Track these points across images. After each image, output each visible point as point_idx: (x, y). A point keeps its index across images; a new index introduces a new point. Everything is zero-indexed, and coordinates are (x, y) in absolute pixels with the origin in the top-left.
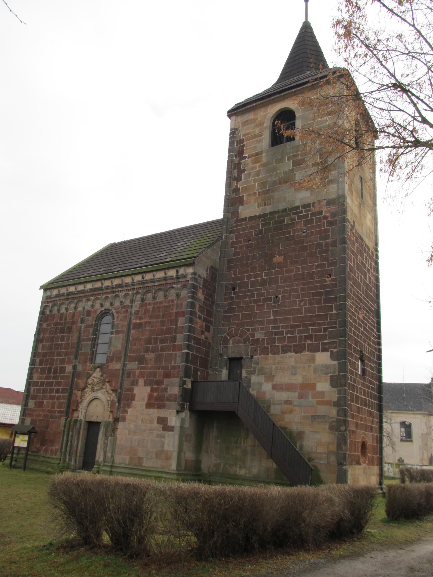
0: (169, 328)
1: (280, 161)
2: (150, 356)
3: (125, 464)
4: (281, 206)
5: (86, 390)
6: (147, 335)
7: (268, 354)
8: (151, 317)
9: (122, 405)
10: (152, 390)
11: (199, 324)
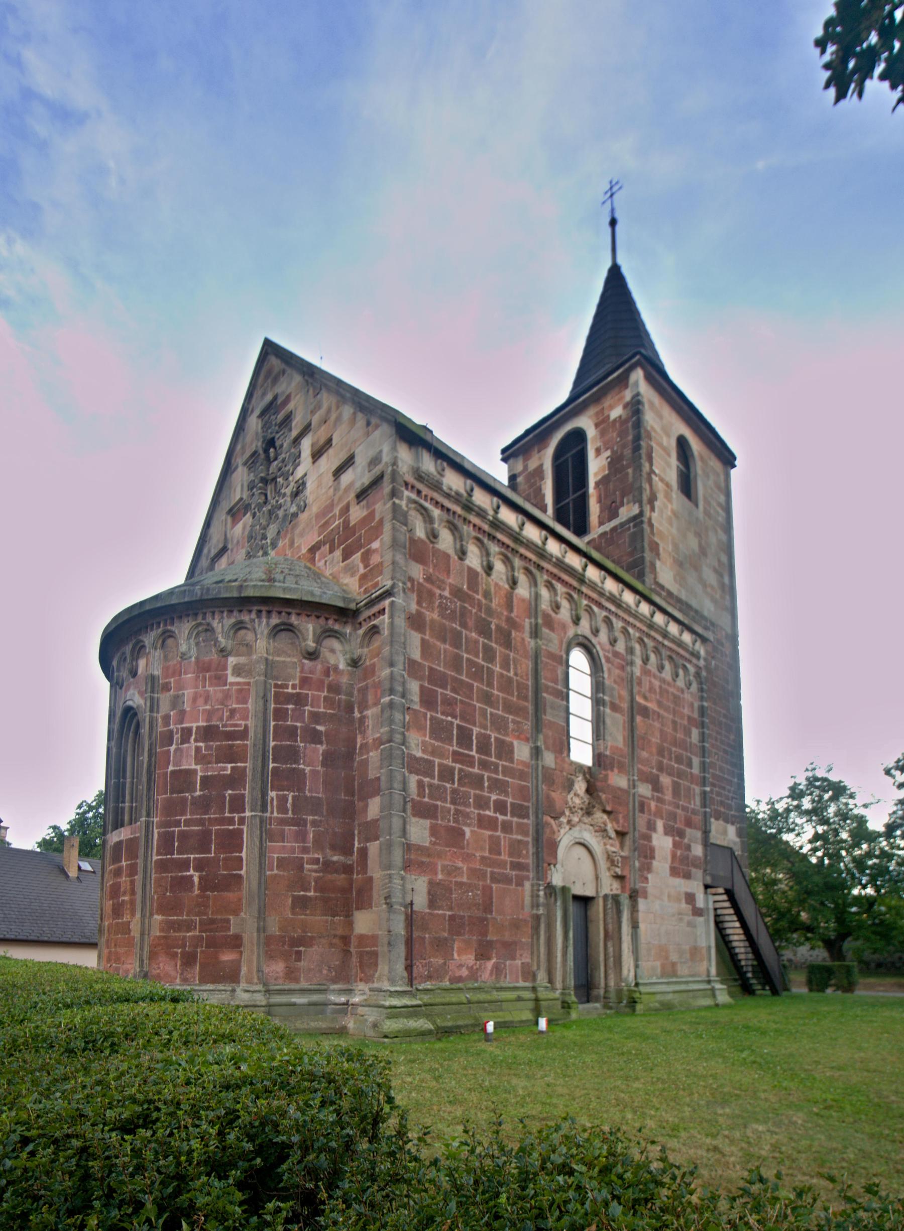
10: (676, 845)
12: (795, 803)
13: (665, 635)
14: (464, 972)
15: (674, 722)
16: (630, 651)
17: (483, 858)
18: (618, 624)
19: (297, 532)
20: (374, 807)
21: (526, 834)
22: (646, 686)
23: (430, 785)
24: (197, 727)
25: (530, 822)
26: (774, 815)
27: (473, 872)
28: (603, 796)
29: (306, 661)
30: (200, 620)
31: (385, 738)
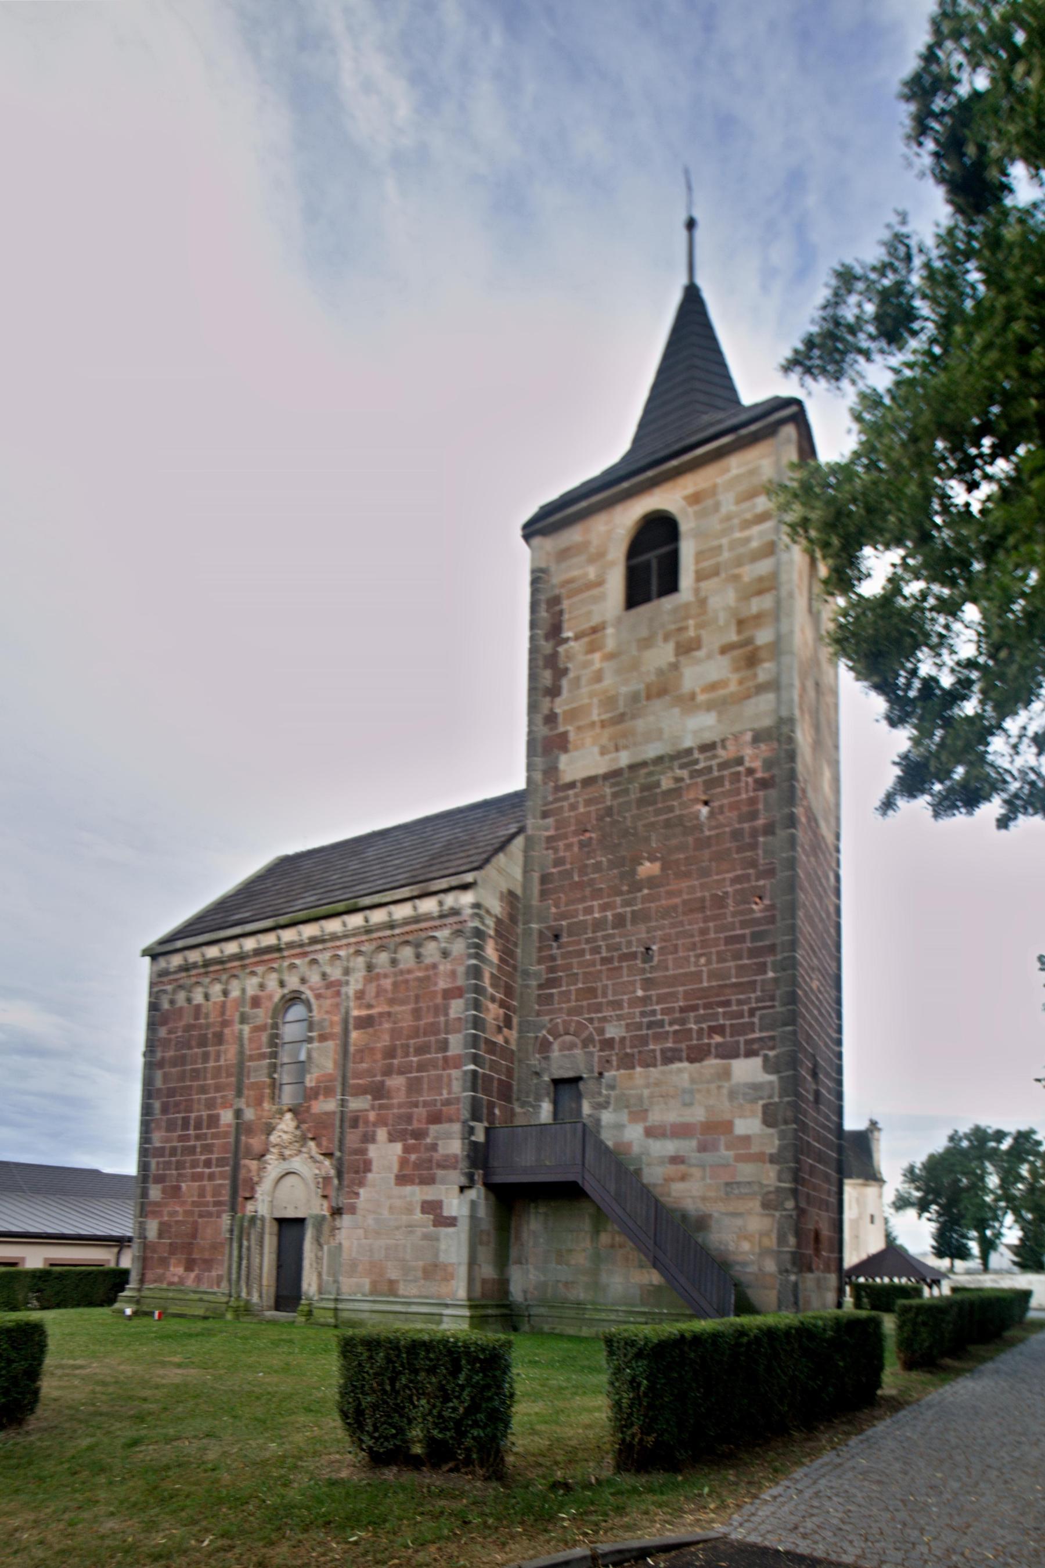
0: (432, 1024)
1: (646, 643)
2: (397, 1082)
3: (364, 1295)
4: (652, 751)
5: (268, 1157)
6: (385, 1041)
7: (633, 1068)
8: (392, 1002)
9: (346, 1183)
10: (407, 1150)
11: (493, 1012)
14: (176, 1279)
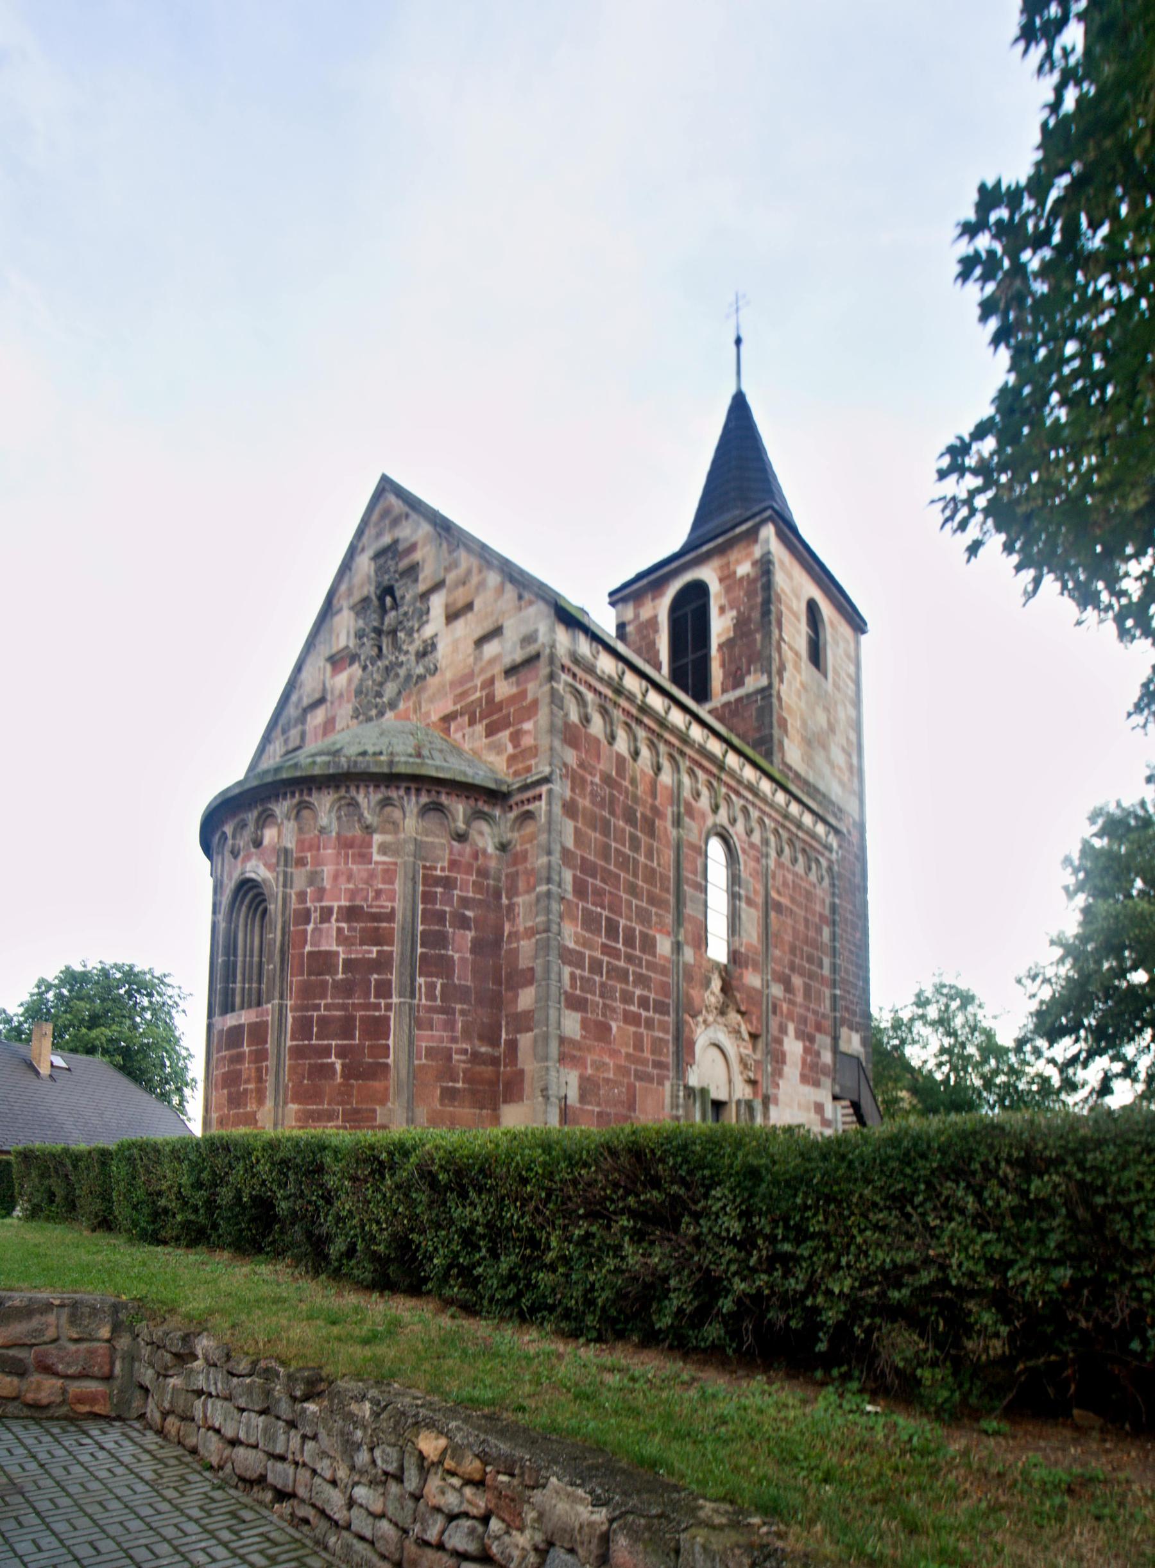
10: (806, 1050)
12: (920, 1011)
13: (799, 826)
15: (806, 920)
16: (766, 842)
17: (628, 1055)
18: (755, 814)
19: (425, 696)
20: (526, 998)
21: (666, 1032)
22: (779, 881)
23: (582, 978)
24: (340, 908)
25: (670, 1019)
26: (897, 1025)
27: (619, 1068)
28: (738, 996)
29: (455, 843)
30: (343, 792)
31: (541, 927)
